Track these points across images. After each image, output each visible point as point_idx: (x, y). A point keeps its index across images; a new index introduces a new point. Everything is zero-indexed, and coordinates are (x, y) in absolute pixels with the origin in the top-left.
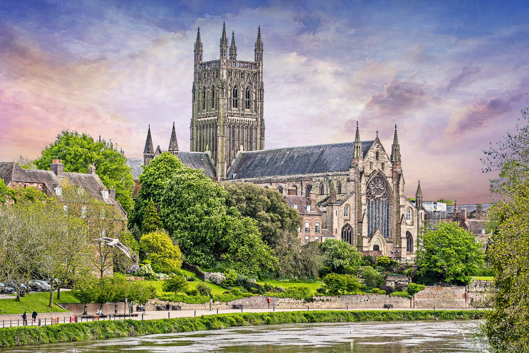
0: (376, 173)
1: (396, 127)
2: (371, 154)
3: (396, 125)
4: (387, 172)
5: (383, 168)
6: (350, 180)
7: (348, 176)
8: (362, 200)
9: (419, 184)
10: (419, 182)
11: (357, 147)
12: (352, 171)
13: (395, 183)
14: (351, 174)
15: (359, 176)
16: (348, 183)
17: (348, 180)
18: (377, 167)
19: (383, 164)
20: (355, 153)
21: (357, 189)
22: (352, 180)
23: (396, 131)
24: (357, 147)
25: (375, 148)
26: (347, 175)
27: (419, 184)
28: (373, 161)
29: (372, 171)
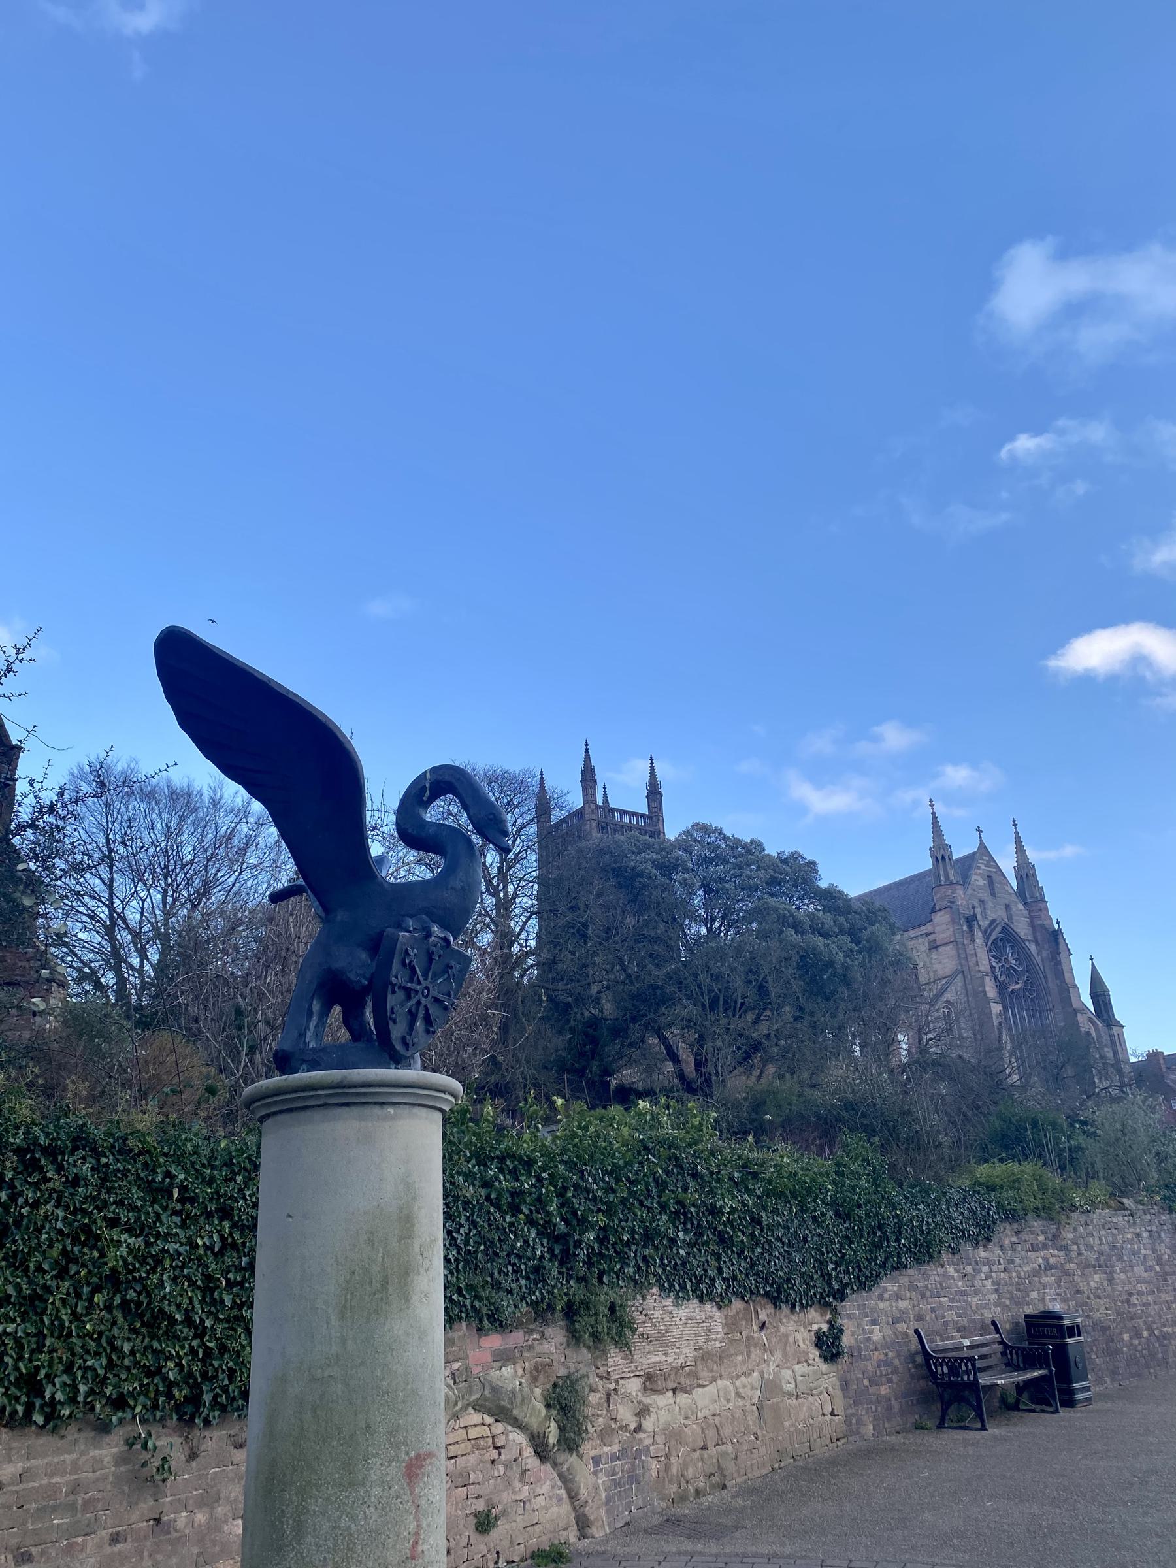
0: (999, 929)
1: (1015, 825)
2: (978, 880)
3: (1014, 821)
4: (1022, 928)
5: (1010, 917)
6: (938, 944)
7: (931, 937)
8: (987, 989)
9: (1093, 964)
10: (1092, 959)
11: (943, 857)
12: (941, 918)
13: (1045, 954)
14: (937, 929)
15: (965, 928)
16: (934, 952)
17: (934, 947)
18: (995, 912)
19: (1007, 906)
20: (942, 873)
21: (963, 962)
22: (946, 941)
23: (1016, 833)
24: (943, 857)
25: (983, 867)
26: (927, 935)
27: (1093, 964)
28: (986, 899)
29: (987, 923)
